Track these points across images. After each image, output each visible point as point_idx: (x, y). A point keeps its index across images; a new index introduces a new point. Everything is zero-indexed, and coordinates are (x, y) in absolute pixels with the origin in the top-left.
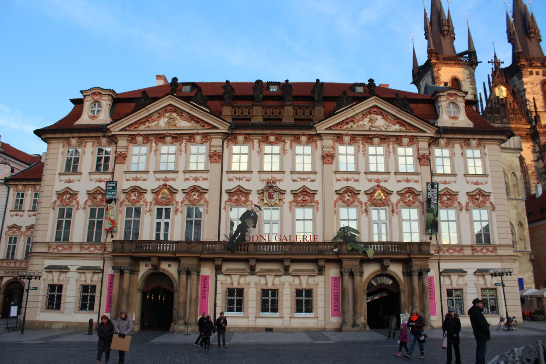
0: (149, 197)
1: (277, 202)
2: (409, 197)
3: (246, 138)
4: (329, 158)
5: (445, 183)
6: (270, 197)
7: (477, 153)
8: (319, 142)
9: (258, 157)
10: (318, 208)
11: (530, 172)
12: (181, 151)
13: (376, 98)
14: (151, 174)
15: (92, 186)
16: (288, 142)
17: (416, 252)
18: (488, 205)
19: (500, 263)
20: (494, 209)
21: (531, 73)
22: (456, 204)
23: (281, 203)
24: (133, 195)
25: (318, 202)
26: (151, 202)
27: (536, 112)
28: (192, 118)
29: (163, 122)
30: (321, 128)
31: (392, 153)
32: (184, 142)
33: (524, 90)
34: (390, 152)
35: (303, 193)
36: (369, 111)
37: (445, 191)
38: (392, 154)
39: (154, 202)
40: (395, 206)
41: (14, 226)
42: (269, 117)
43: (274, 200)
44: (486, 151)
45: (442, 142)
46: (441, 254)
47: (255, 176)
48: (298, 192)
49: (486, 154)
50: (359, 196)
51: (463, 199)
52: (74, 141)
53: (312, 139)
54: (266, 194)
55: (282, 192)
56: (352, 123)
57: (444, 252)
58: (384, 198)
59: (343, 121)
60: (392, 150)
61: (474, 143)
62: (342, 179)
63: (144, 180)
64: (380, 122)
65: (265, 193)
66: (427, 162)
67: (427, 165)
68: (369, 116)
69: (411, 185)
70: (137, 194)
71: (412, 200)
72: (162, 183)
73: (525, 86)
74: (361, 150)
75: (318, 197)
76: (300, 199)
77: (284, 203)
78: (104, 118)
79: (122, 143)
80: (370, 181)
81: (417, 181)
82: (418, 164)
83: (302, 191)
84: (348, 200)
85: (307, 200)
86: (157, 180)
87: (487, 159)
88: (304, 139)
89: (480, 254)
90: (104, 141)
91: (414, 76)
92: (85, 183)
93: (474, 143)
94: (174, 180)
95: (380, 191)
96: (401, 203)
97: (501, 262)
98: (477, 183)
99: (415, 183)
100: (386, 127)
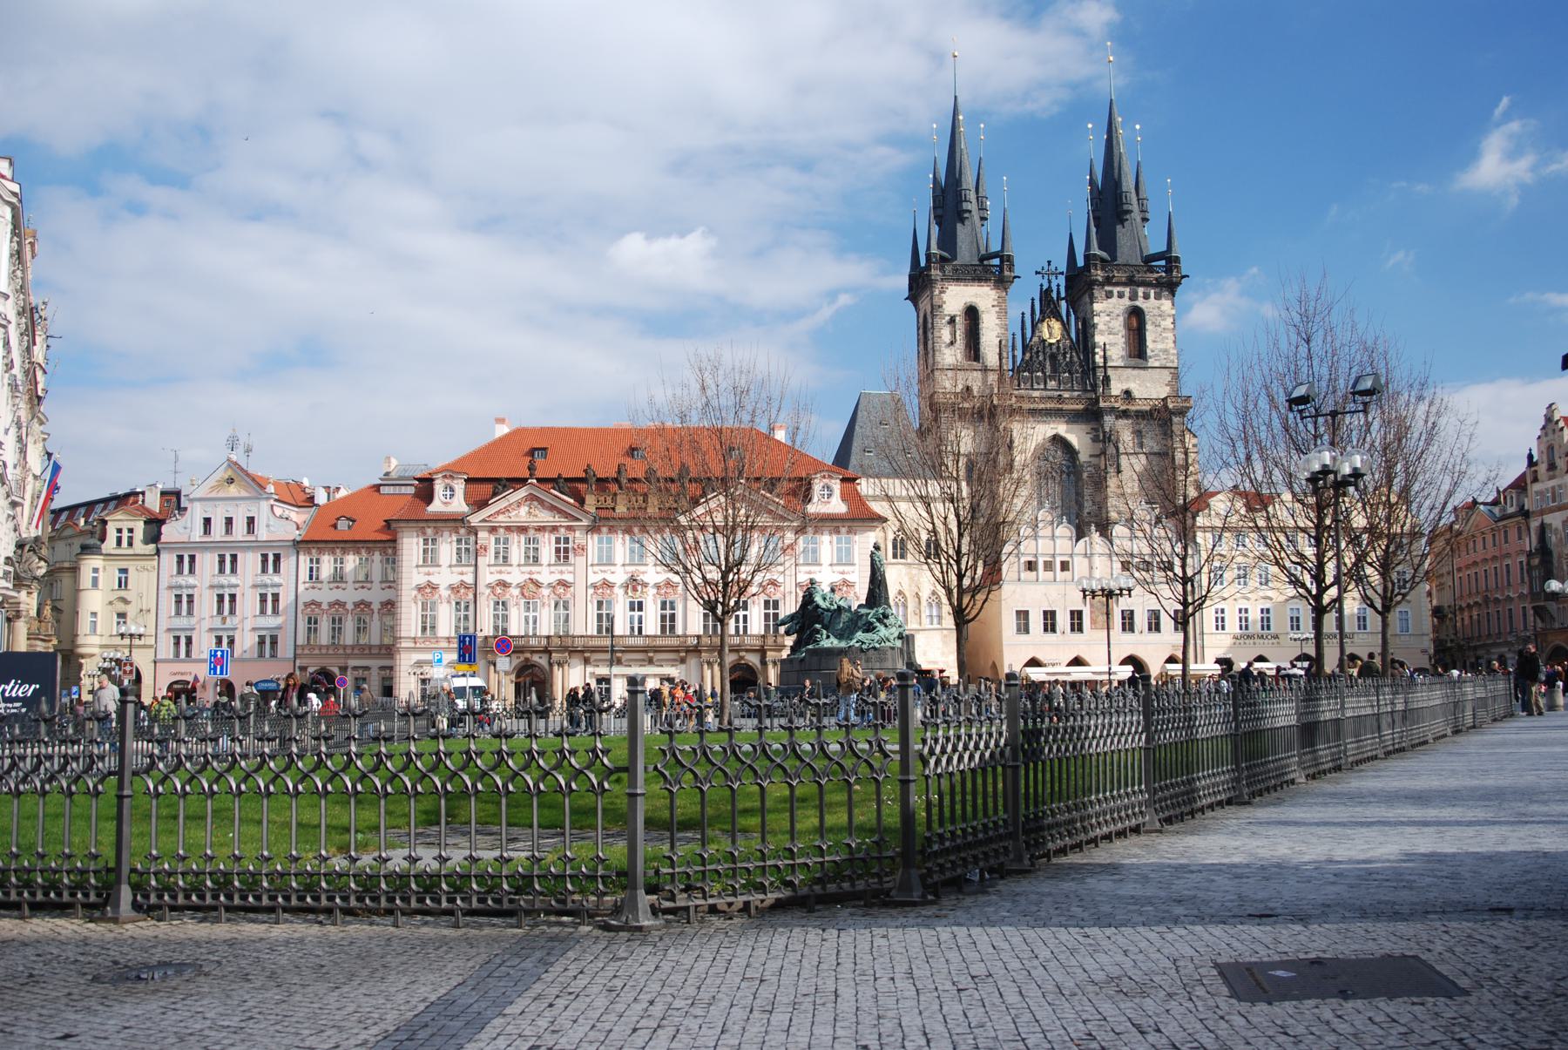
6: (635, 589)
11: (1085, 475)
15: (455, 579)
21: (1109, 295)
27: (1105, 367)
28: (553, 508)
29: (524, 510)
33: (1094, 326)
41: (313, 603)
45: (810, 529)
47: (619, 569)
52: (429, 531)
53: (679, 530)
55: (645, 585)
61: (843, 530)
73: (1096, 320)
78: (459, 505)
79: (482, 535)
90: (462, 531)
91: (911, 288)
92: (446, 575)
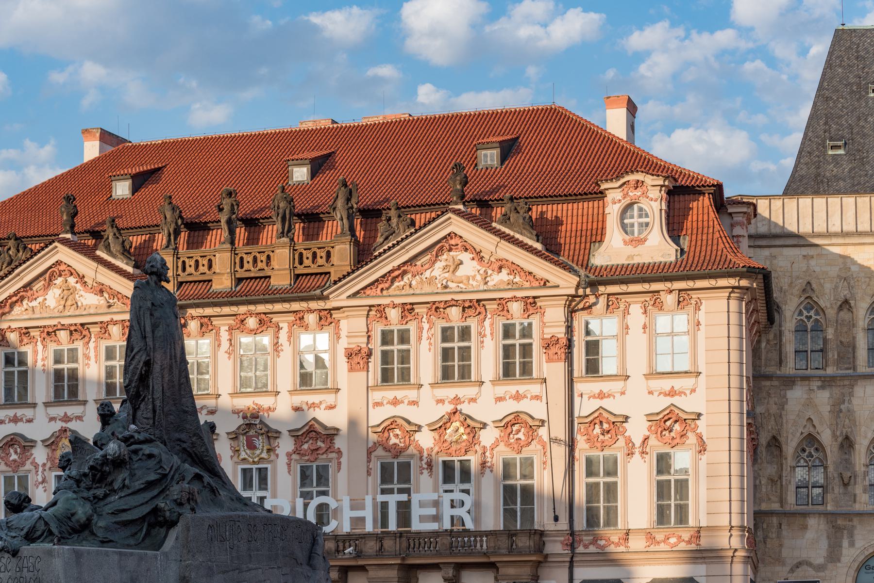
0: (40, 455)
1: (264, 455)
2: (518, 431)
3: (202, 325)
4: (357, 359)
5: (601, 396)
6: (251, 446)
7: (682, 321)
8: (343, 324)
9: (231, 362)
10: (339, 464)
12: (88, 358)
13: (450, 218)
14: (40, 408)
16: (285, 326)
17: (504, 551)
18: (692, 439)
19: (704, 566)
20: (702, 448)
22: (621, 442)
23: (273, 457)
24: (12, 451)
25: (339, 452)
26: (44, 465)
30: (339, 298)
31: (489, 336)
32: (93, 339)
34: (485, 336)
35: (311, 435)
36: (438, 248)
37: (596, 415)
38: (488, 340)
39: (49, 465)
40: (487, 454)
42: (247, 275)
43: (258, 452)
44: (702, 316)
46: (580, 549)
48: (300, 433)
49: (698, 324)
50: (417, 436)
51: (637, 430)
54: (243, 439)
55: (271, 435)
56: (410, 276)
57: (586, 547)
58: (465, 437)
59: (383, 276)
60: (488, 332)
62: (385, 402)
63: (30, 421)
64: (469, 267)
65: (241, 437)
66: (562, 353)
67: (559, 360)
68: (445, 257)
69: (525, 406)
70: (19, 450)
71: (523, 438)
72: (58, 426)
74: (425, 335)
75: (339, 443)
76: (306, 446)
77: (277, 456)
80: (440, 401)
81: (537, 397)
82: (544, 357)
83: (309, 432)
84: (395, 444)
85: (317, 449)
86: (52, 419)
87: (701, 334)
88: (311, 319)
89: (663, 547)
93: (670, 300)
94: (79, 418)
95: (457, 424)
96: (502, 447)
97: (705, 563)
98: (672, 393)
99: (534, 402)
100: (479, 278)
